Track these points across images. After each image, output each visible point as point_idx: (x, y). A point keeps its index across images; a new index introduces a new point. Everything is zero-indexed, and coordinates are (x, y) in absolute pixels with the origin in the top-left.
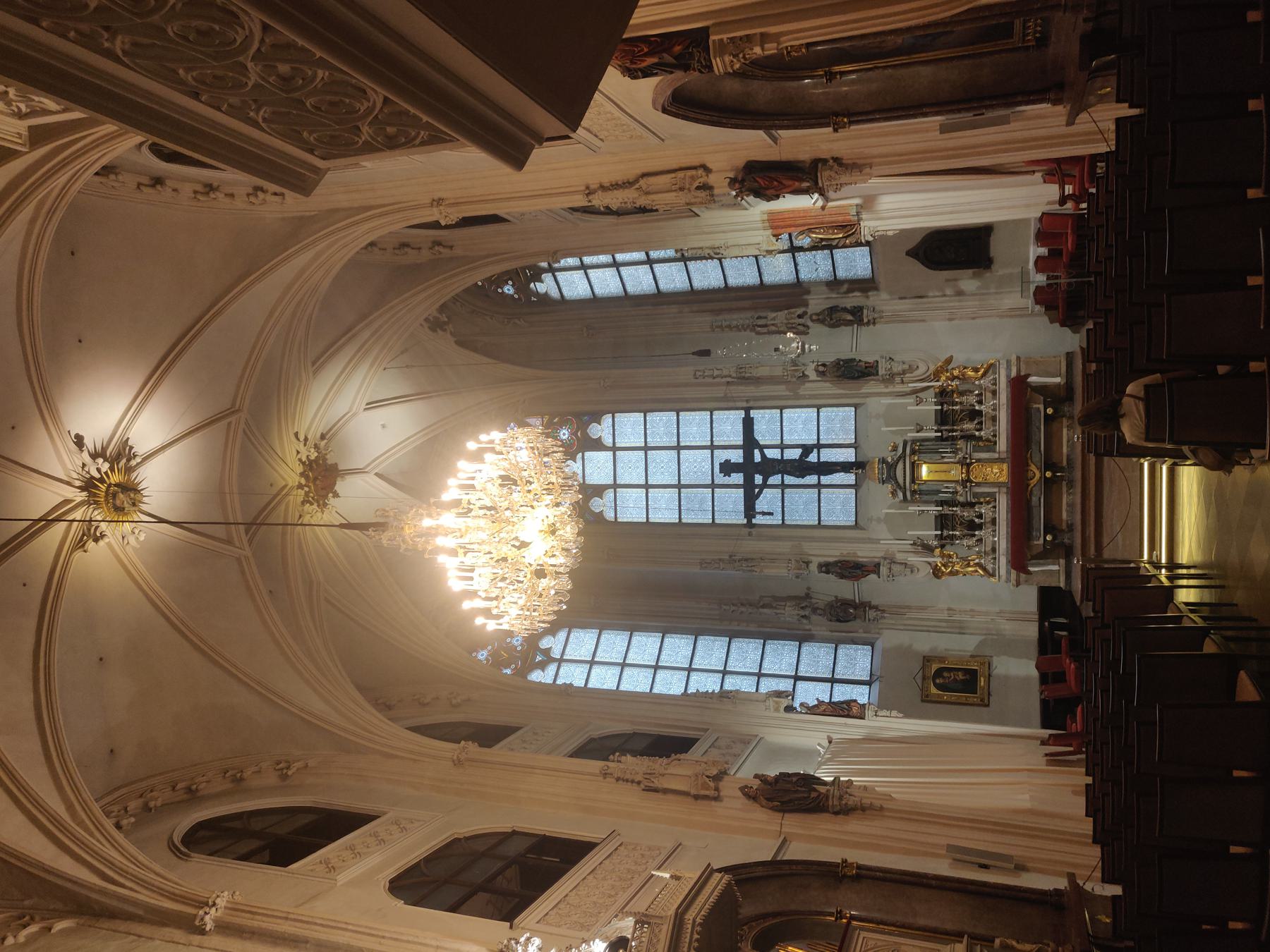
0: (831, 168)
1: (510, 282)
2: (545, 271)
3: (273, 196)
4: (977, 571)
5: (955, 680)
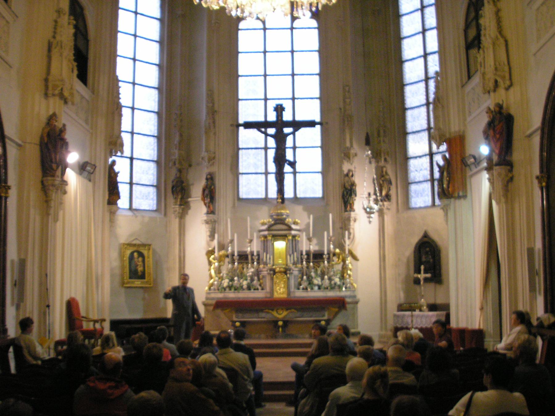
0: (507, 175)
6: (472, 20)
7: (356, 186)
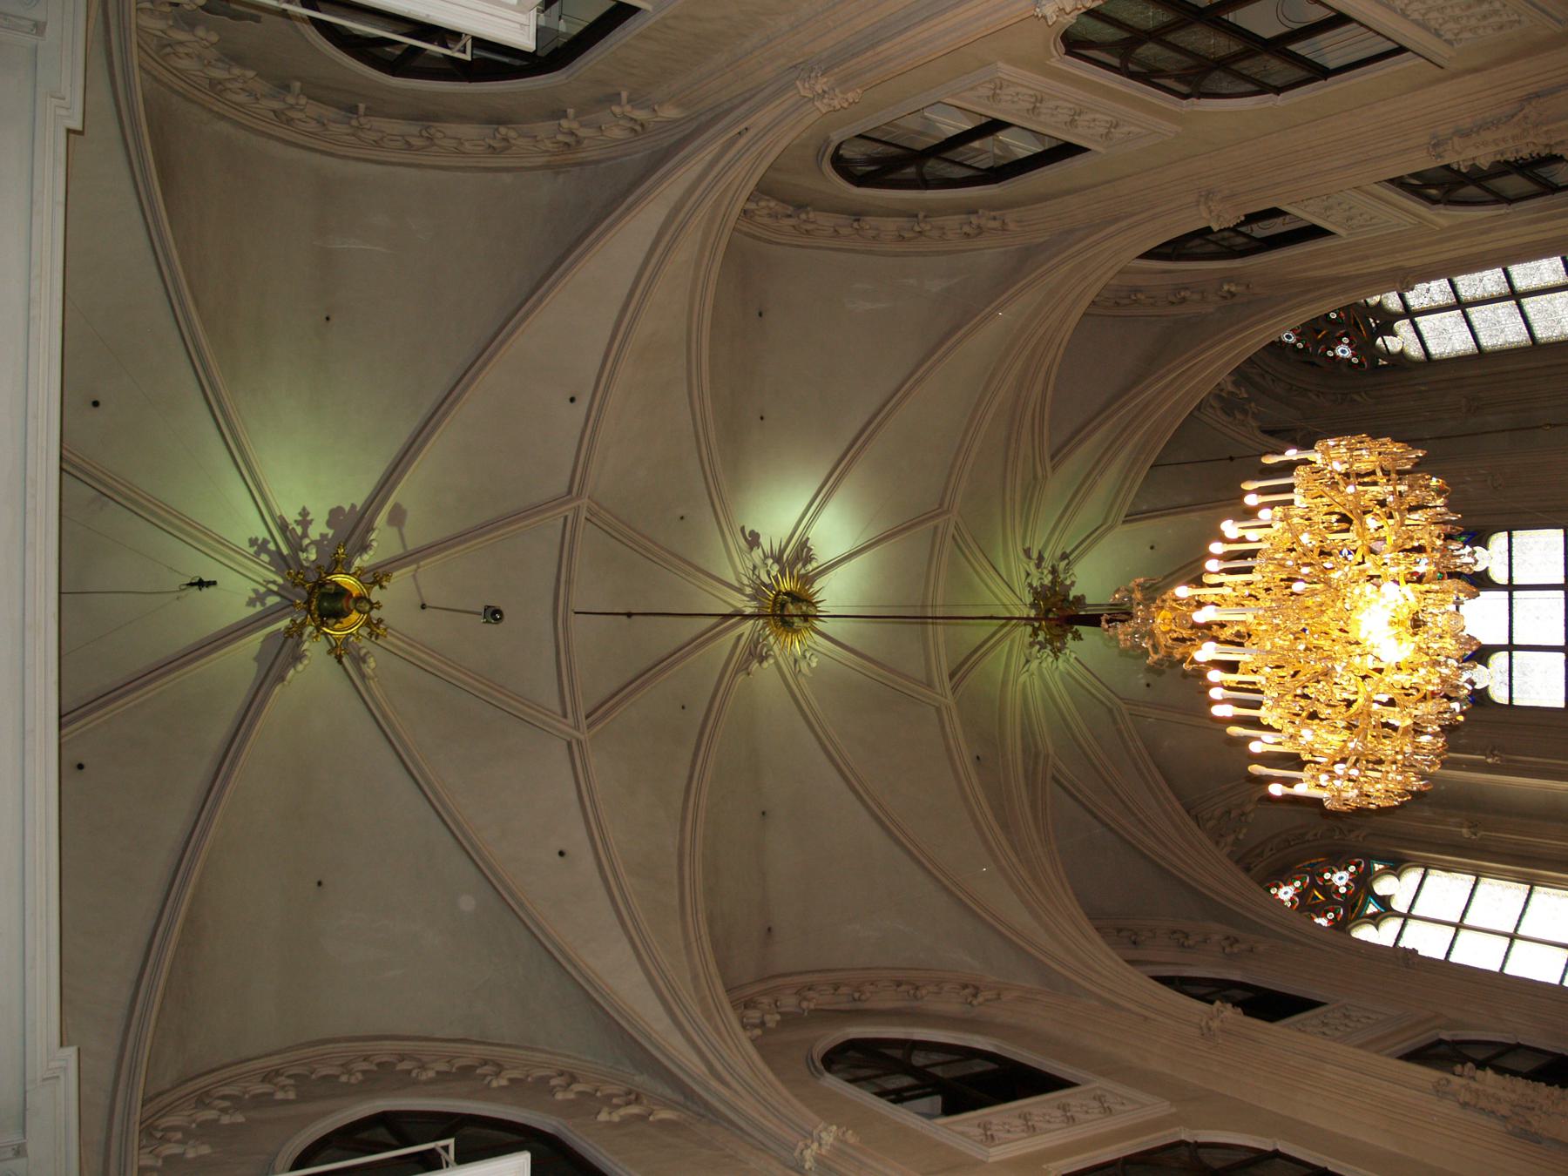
1: (1345, 340)
2: (1399, 317)
6: (1487, 190)
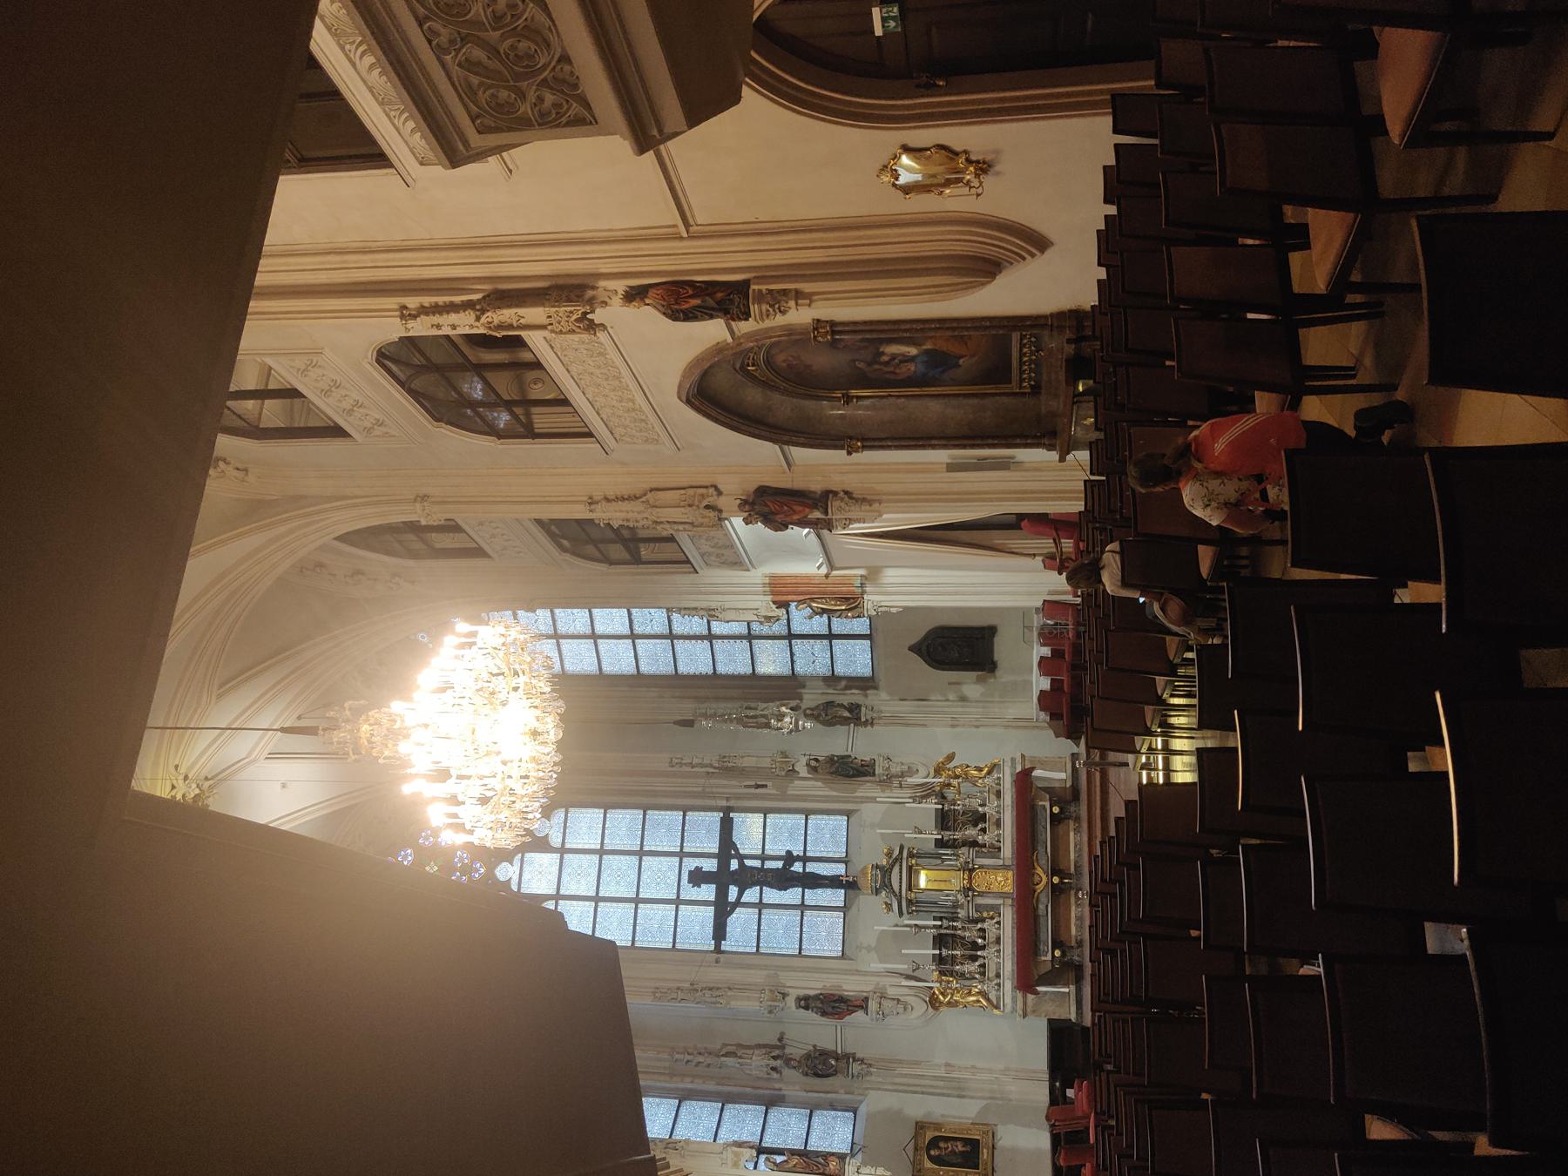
3: (236, 471)
4: (978, 1001)
5: (953, 1152)
7: (833, 756)
